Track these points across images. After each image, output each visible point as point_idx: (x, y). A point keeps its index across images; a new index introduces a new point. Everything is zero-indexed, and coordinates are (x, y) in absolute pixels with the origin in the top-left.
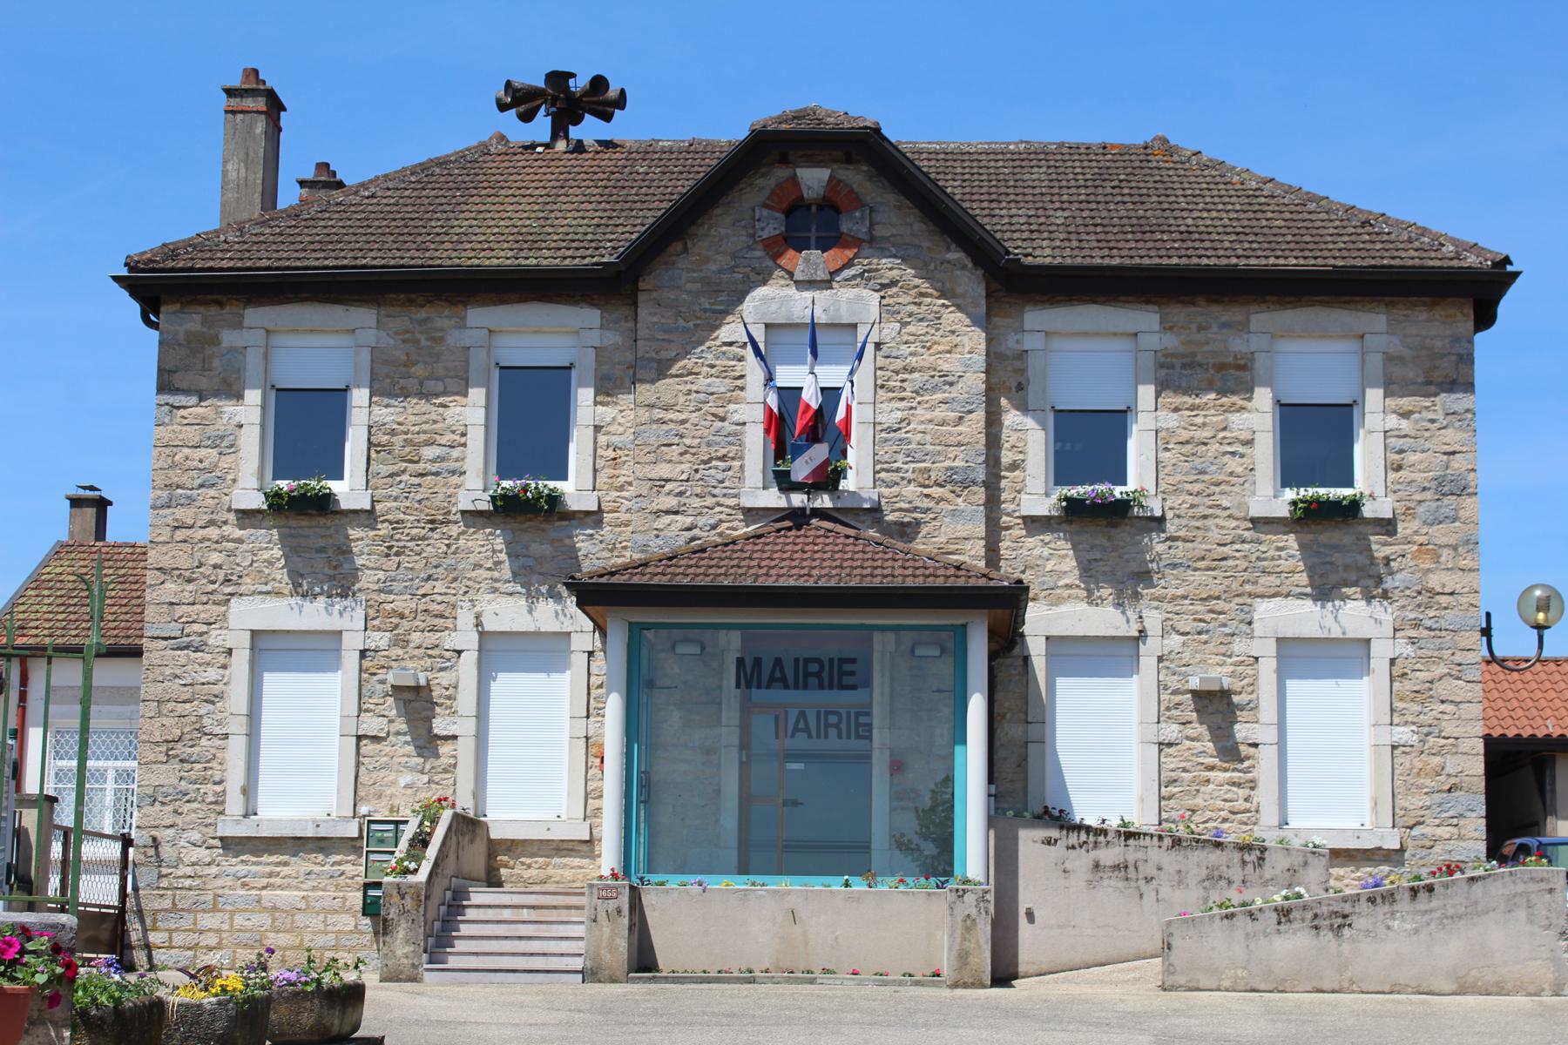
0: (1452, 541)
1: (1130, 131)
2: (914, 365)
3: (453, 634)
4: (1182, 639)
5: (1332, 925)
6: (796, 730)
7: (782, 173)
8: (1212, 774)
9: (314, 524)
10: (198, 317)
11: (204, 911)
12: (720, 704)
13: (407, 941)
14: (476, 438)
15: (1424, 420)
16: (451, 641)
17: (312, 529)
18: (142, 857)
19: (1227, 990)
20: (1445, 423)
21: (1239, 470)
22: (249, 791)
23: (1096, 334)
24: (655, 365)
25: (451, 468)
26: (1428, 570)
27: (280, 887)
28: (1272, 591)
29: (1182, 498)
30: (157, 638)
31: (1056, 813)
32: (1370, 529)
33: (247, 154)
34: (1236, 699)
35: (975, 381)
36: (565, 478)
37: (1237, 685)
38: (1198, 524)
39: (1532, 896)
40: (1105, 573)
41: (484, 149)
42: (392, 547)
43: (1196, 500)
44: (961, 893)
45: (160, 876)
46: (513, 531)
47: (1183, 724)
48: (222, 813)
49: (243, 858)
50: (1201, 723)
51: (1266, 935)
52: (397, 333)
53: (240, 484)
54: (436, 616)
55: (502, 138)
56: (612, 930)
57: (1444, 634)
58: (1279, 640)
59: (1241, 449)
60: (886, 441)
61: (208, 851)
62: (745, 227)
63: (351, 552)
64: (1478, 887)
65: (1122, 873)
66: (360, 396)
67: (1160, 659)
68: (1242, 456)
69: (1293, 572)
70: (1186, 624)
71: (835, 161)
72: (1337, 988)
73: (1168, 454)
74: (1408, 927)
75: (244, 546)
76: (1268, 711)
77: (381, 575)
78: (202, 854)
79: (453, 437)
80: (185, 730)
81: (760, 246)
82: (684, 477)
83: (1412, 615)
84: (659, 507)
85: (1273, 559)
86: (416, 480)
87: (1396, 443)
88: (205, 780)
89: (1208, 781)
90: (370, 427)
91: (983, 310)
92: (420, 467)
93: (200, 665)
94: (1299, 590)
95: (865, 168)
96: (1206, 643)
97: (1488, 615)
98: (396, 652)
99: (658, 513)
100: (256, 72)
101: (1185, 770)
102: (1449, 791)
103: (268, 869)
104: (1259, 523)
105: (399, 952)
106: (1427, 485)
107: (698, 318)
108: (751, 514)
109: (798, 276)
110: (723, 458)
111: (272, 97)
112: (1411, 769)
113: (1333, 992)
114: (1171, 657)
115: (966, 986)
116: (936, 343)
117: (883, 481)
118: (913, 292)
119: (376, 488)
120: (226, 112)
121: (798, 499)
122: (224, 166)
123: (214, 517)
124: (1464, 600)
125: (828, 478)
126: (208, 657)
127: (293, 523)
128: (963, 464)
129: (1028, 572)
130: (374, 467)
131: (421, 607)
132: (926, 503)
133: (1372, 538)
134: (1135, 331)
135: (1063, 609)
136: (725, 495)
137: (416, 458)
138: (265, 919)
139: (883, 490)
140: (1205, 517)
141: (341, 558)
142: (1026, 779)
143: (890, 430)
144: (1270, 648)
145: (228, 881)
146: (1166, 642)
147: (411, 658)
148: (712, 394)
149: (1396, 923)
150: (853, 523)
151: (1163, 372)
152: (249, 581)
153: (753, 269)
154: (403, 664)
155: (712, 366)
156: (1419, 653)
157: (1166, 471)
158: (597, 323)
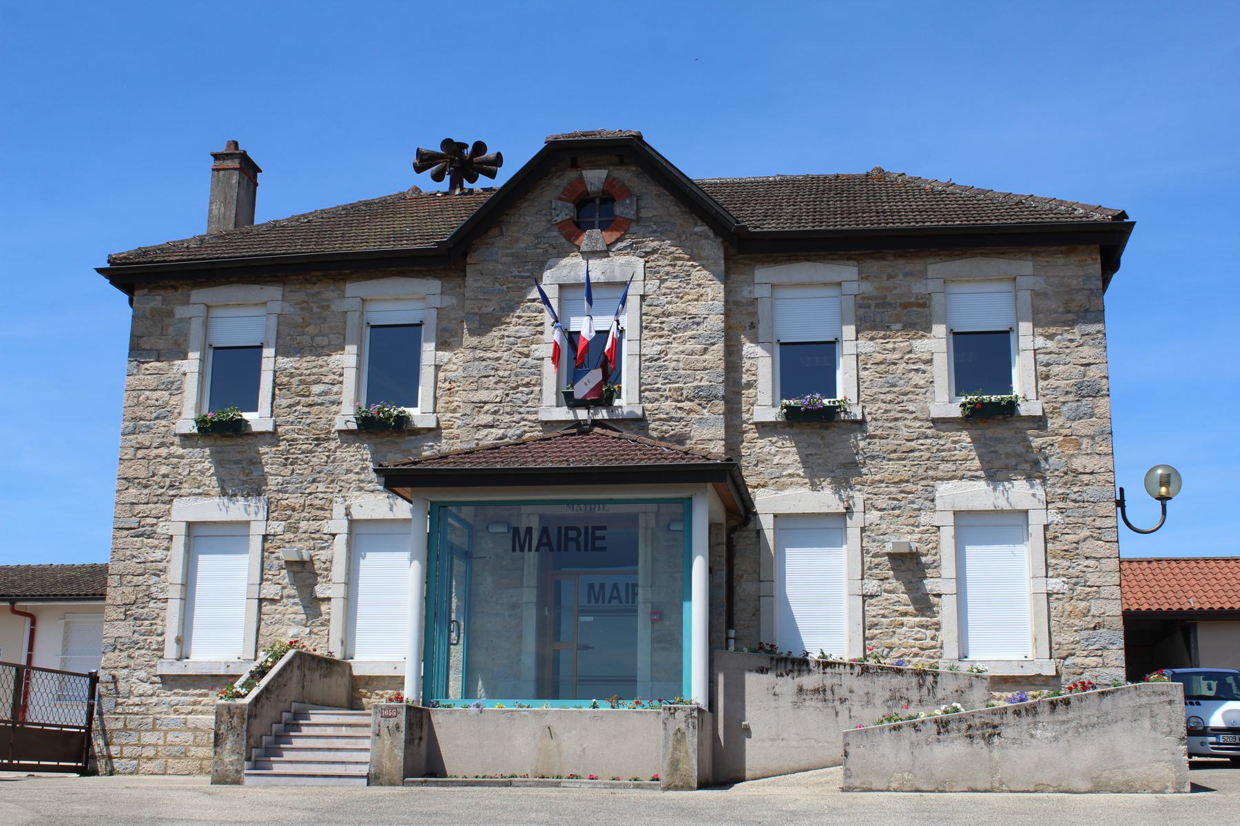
1: (854, 165)
2: (670, 310)
3: (330, 522)
5: (984, 735)
6: (612, 598)
7: (572, 175)
8: (905, 619)
9: (234, 443)
10: (159, 298)
11: (146, 730)
12: (523, 570)
13: (233, 752)
14: (350, 377)
15: (1064, 340)
16: (328, 527)
17: (233, 447)
18: (105, 690)
19: (895, 791)
20: (1081, 341)
21: (922, 382)
22: (182, 641)
23: (811, 285)
24: (478, 317)
25: (332, 400)
26: (1072, 455)
27: (202, 713)
28: (950, 475)
29: (878, 405)
30: (122, 529)
32: (1026, 425)
33: (226, 198)
34: (924, 559)
35: (716, 321)
36: (415, 405)
37: (923, 548)
38: (891, 425)
39: (1155, 708)
40: (819, 465)
41: (402, 197)
42: (288, 458)
43: (889, 407)
44: (672, 711)
45: (117, 704)
46: (375, 444)
47: (882, 580)
48: (161, 657)
49: (175, 691)
50: (897, 580)
51: (928, 743)
52: (297, 304)
53: (183, 416)
54: (318, 509)
55: (417, 190)
56: (392, 743)
57: (1086, 504)
58: (955, 513)
59: (923, 367)
60: (649, 368)
61: (151, 686)
63: (261, 463)
64: (1108, 700)
65: (821, 696)
66: (269, 352)
67: (863, 530)
68: (924, 372)
69: (966, 460)
70: (882, 502)
72: (988, 787)
73: (866, 373)
74: (1049, 735)
75: (185, 461)
76: (948, 567)
77: (280, 479)
78: (147, 688)
79: (333, 377)
80: (139, 596)
81: (556, 228)
82: (498, 399)
83: (1060, 491)
84: (480, 422)
85: (950, 450)
86: (307, 410)
87: (1043, 358)
88: (151, 633)
89: (902, 624)
90: (275, 372)
91: (722, 267)
92: (310, 400)
93: (151, 548)
94: (970, 473)
95: (634, 169)
96: (898, 516)
97: (1122, 490)
99: (478, 427)
100: (236, 144)
101: (884, 616)
102: (1094, 628)
103: (193, 699)
104: (937, 422)
105: (227, 760)
106: (1069, 389)
107: (510, 282)
108: (546, 424)
109: (584, 248)
110: (527, 385)
111: (244, 158)
112: (1063, 612)
113: (986, 791)
114: (872, 528)
115: (676, 788)
116: (686, 294)
117: (647, 398)
118: (669, 257)
119: (278, 416)
120: (213, 170)
121: (582, 414)
122: (210, 206)
123: (164, 440)
124: (1102, 478)
125: (604, 396)
126: (156, 542)
127: (219, 443)
128: (708, 383)
129: (760, 465)
130: (278, 401)
131: (308, 502)
132: (680, 414)
133: (1029, 432)
134: (839, 280)
135: (787, 492)
136: (528, 412)
137: (307, 393)
138: (188, 737)
139: (646, 405)
140: (896, 419)
141: (252, 467)
142: (759, 625)
143: (652, 360)
144: (949, 519)
145: (164, 708)
146: (867, 516)
147: (299, 540)
148: (520, 337)
149: (1039, 731)
151: (862, 311)
152: (187, 486)
153: (551, 245)
154: (293, 544)
155: (520, 317)
156: (1067, 520)
157: (865, 385)
158: (439, 291)
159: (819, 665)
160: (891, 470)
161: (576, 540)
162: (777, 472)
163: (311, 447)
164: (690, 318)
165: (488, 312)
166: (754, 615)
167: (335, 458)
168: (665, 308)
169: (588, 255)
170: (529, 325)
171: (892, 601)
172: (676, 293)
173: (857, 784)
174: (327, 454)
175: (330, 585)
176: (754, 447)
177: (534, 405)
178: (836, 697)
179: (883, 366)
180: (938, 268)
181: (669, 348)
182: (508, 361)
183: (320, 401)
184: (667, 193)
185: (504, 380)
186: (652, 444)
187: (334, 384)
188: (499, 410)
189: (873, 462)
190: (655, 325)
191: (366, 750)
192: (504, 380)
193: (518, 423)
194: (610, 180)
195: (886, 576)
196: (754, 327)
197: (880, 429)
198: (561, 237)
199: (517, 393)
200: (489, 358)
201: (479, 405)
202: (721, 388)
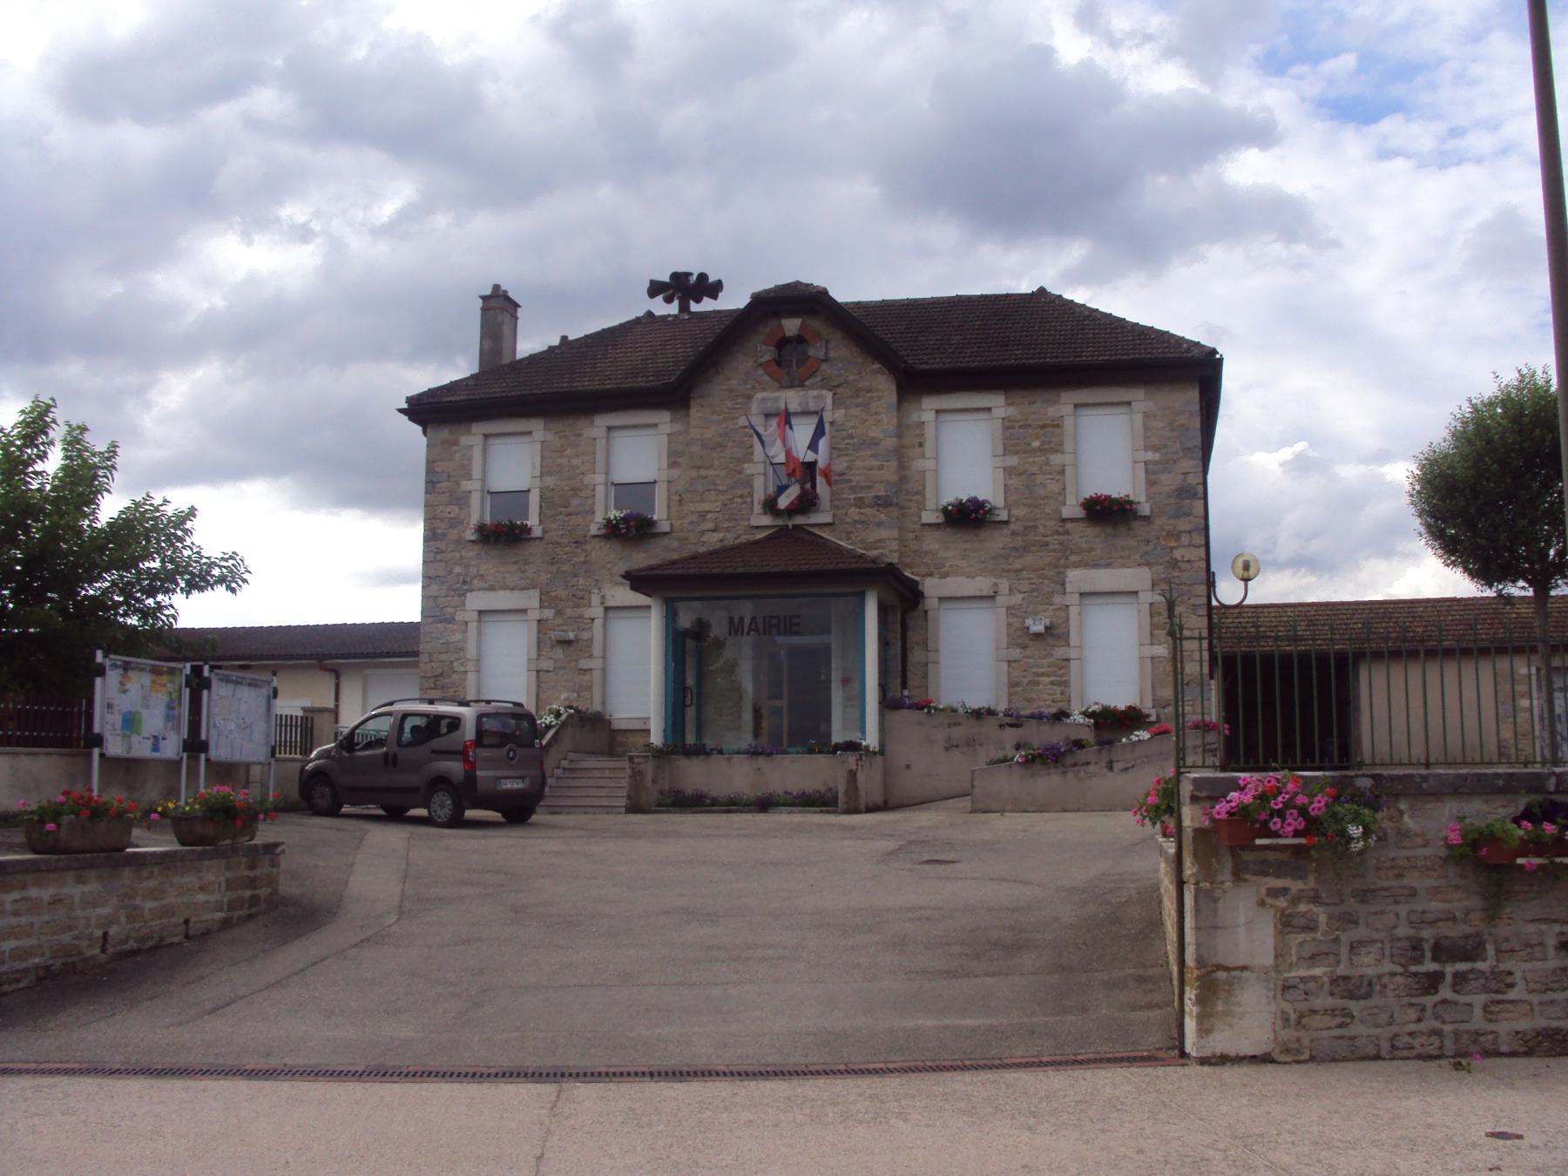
0: (1187, 527)
4: (1022, 595)
16: (589, 613)
41: (638, 321)
52: (556, 433)
55: (650, 314)
86: (566, 519)
92: (570, 509)
98: (558, 621)
101: (1024, 676)
128: (883, 493)
153: (757, 382)
163: (571, 549)
180: (1069, 398)
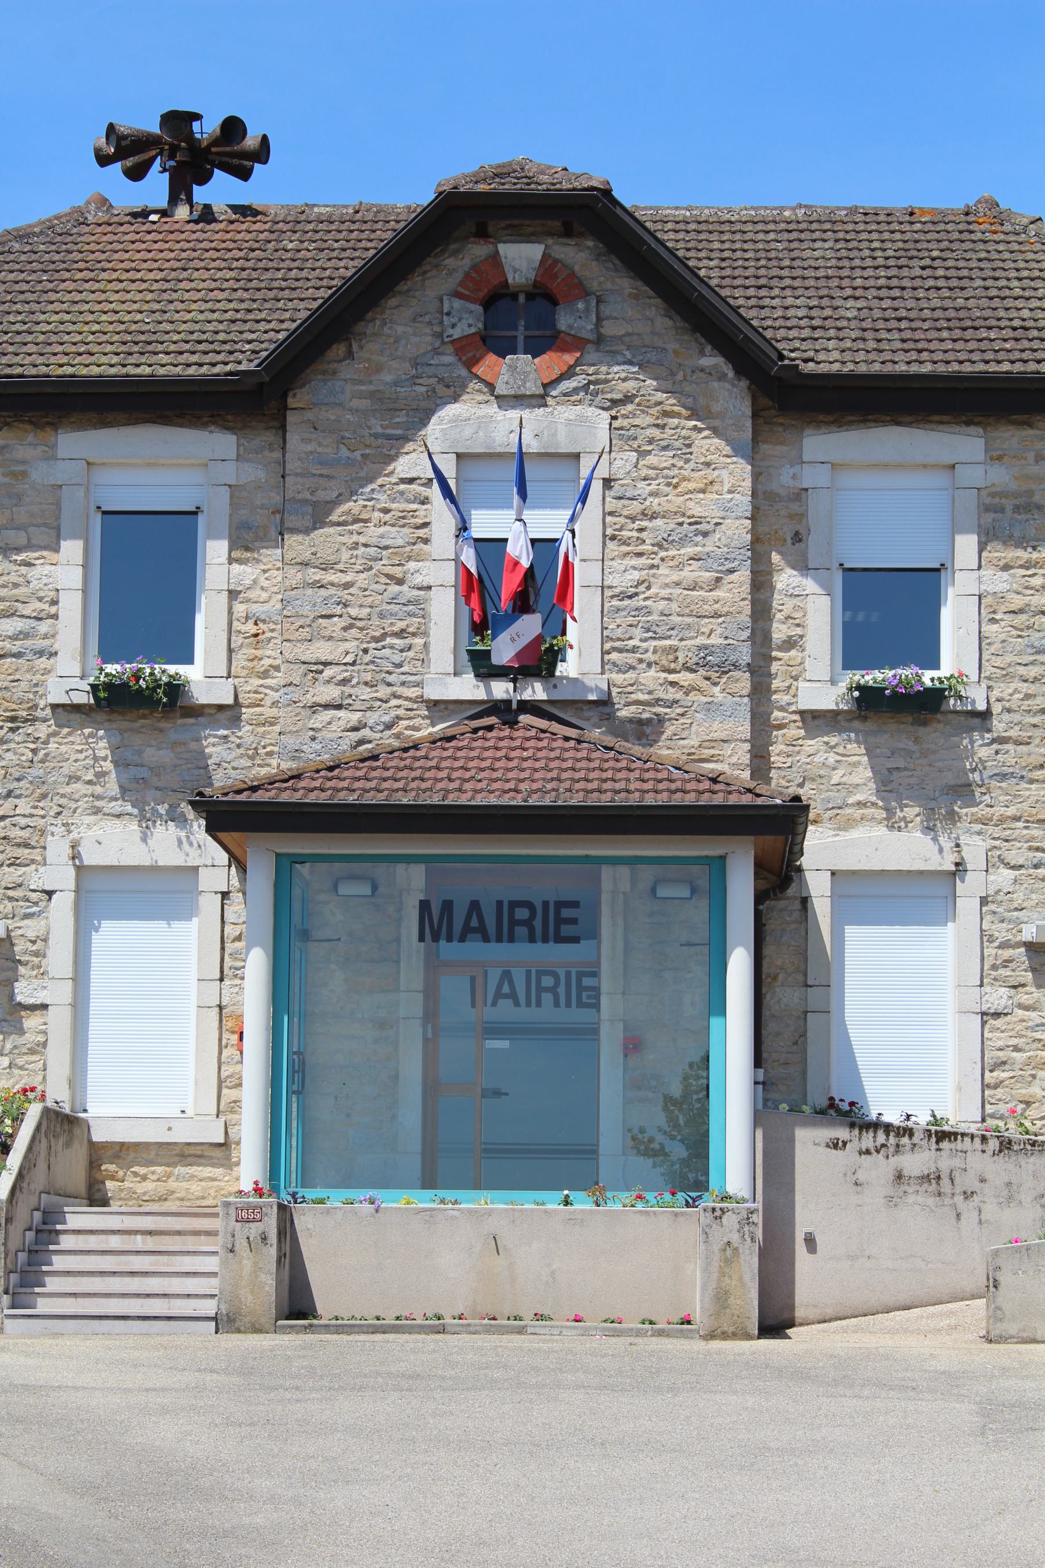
2: (656, 508)
3: (42, 869)
4: (1012, 874)
6: (498, 995)
7: (479, 250)
12: (398, 962)
14: (71, 607)
23: (899, 466)
24: (310, 509)
29: (1013, 686)
31: (845, 1107)
36: (189, 660)
40: (910, 787)
43: (1032, 689)
44: (718, 1213)
46: (121, 732)
47: (1015, 987)
54: (19, 845)
55: (103, 202)
56: (255, 1263)
62: (430, 323)
67: (984, 901)
70: (1017, 854)
71: (550, 234)
73: (995, 627)
81: (450, 349)
82: (349, 659)
91: (749, 434)
95: (590, 244)
99: (315, 707)
101: (1017, 1049)
107: (367, 446)
108: (438, 708)
109: (501, 389)
110: (401, 634)
114: (999, 898)
115: (725, 1336)
116: (684, 479)
117: (614, 664)
118: (654, 411)
121: (501, 689)
128: (721, 641)
129: (808, 785)
132: (672, 694)
135: (855, 834)
136: (403, 684)
139: (614, 676)
142: (805, 1061)
143: (623, 596)
146: (991, 878)
148: (386, 548)
150: (573, 720)
151: (989, 517)
153: (441, 380)
155: (386, 511)
157: (992, 650)
159: (930, 1136)
160: (1033, 799)
161: (528, 923)
162: (837, 798)
164: (690, 524)
165: (328, 498)
166: (796, 1043)
167: (47, 755)
168: (647, 503)
169: (505, 401)
170: (403, 526)
171: (1030, 1024)
172: (667, 477)
173: (1013, 1331)
174: (33, 746)
175: (45, 982)
176: (799, 752)
177: (414, 670)
178: (958, 1190)
179: (1023, 617)
181: (654, 576)
182: (365, 590)
183: (15, 649)
184: (652, 293)
185: (360, 624)
186: (645, 757)
187: (40, 619)
188: (352, 677)
189: (1003, 785)
190: (630, 534)
191: (214, 1274)
192: (360, 624)
193: (386, 702)
194: (548, 264)
195: (1023, 981)
196: (800, 540)
197: (1017, 728)
198: (460, 366)
199: (384, 647)
200: (333, 584)
201: (314, 668)
202: (745, 650)
